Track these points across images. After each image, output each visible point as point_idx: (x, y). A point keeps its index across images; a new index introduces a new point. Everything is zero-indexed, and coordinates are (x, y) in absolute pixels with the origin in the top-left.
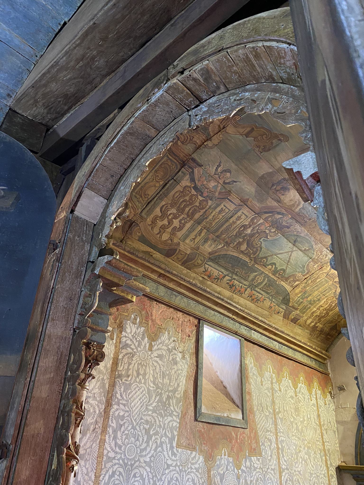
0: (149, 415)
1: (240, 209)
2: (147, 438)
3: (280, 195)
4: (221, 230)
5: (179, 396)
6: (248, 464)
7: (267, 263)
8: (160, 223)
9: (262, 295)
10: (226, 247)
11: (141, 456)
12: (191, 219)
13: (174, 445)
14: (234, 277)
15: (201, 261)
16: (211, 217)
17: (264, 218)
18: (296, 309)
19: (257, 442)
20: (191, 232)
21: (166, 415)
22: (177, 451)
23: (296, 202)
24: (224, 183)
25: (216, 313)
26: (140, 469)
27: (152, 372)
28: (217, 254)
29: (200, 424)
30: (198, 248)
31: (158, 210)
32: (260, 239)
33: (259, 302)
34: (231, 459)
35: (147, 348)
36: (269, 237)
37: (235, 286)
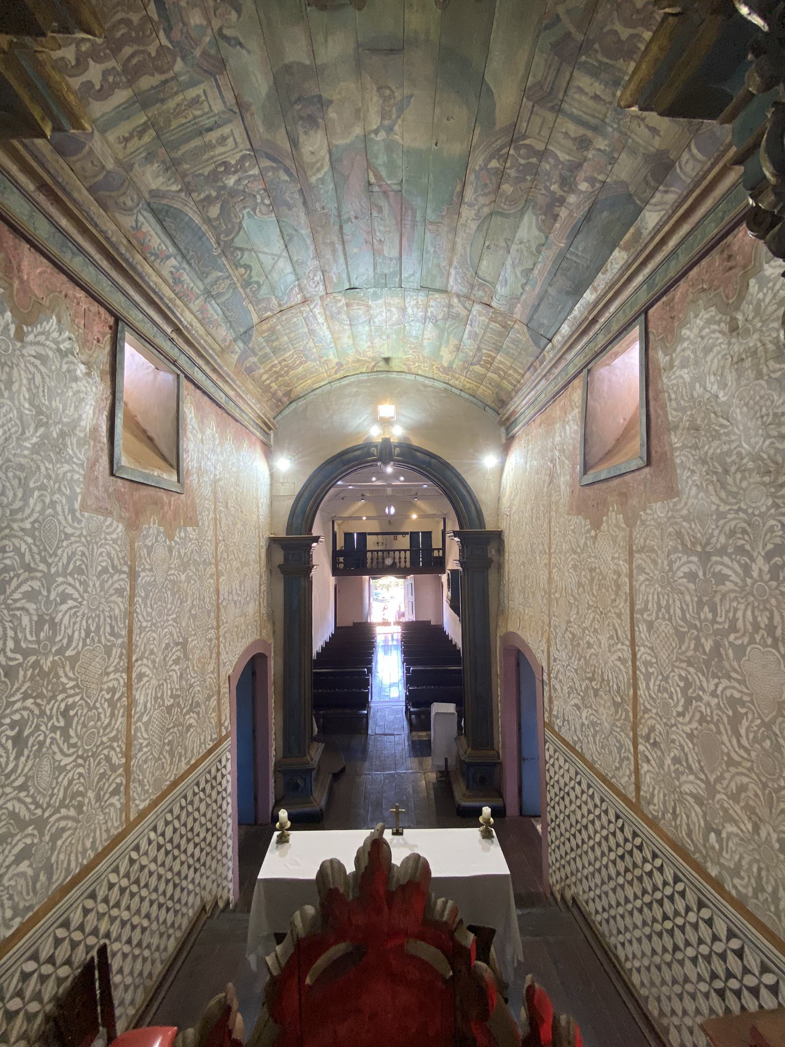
0: (25, 457)
1: (231, 121)
2: (24, 494)
3: (301, 130)
4: (185, 148)
5: (82, 435)
6: (183, 534)
10: (183, 194)
11: (15, 521)
13: (77, 506)
15: (132, 200)
17: (262, 165)
18: (255, 354)
19: (194, 510)
21: (58, 461)
22: (83, 516)
23: (317, 161)
25: (146, 320)
26: (14, 540)
27: (25, 381)
28: (165, 201)
29: (119, 481)
30: (131, 167)
35: (12, 332)
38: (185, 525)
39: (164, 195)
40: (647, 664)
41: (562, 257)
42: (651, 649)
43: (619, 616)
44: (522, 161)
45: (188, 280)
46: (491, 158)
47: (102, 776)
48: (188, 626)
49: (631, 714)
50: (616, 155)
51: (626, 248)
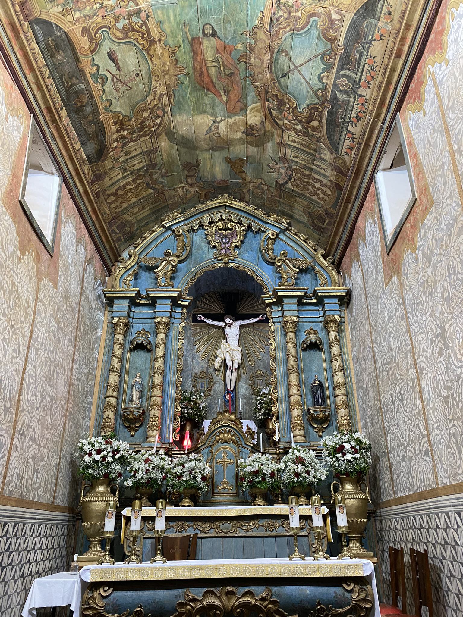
4: (309, 151)
7: (321, 87)
8: (322, 196)
9: (365, 64)
12: (311, 175)
14: (347, 119)
16: (303, 163)
20: (320, 173)
24: (277, 164)
30: (330, 164)
31: (313, 198)
32: (301, 113)
33: (375, 65)
34: (409, 252)
36: (295, 106)
37: (357, 114)
38: (422, 223)
39: (329, 148)
40: (30, 376)
41: (96, 111)
42: (34, 367)
43: (24, 336)
44: (146, 129)
45: (354, 111)
46: (161, 122)
47: (419, 435)
48: (442, 313)
49: (14, 416)
50: (114, 162)
51: (79, 150)
